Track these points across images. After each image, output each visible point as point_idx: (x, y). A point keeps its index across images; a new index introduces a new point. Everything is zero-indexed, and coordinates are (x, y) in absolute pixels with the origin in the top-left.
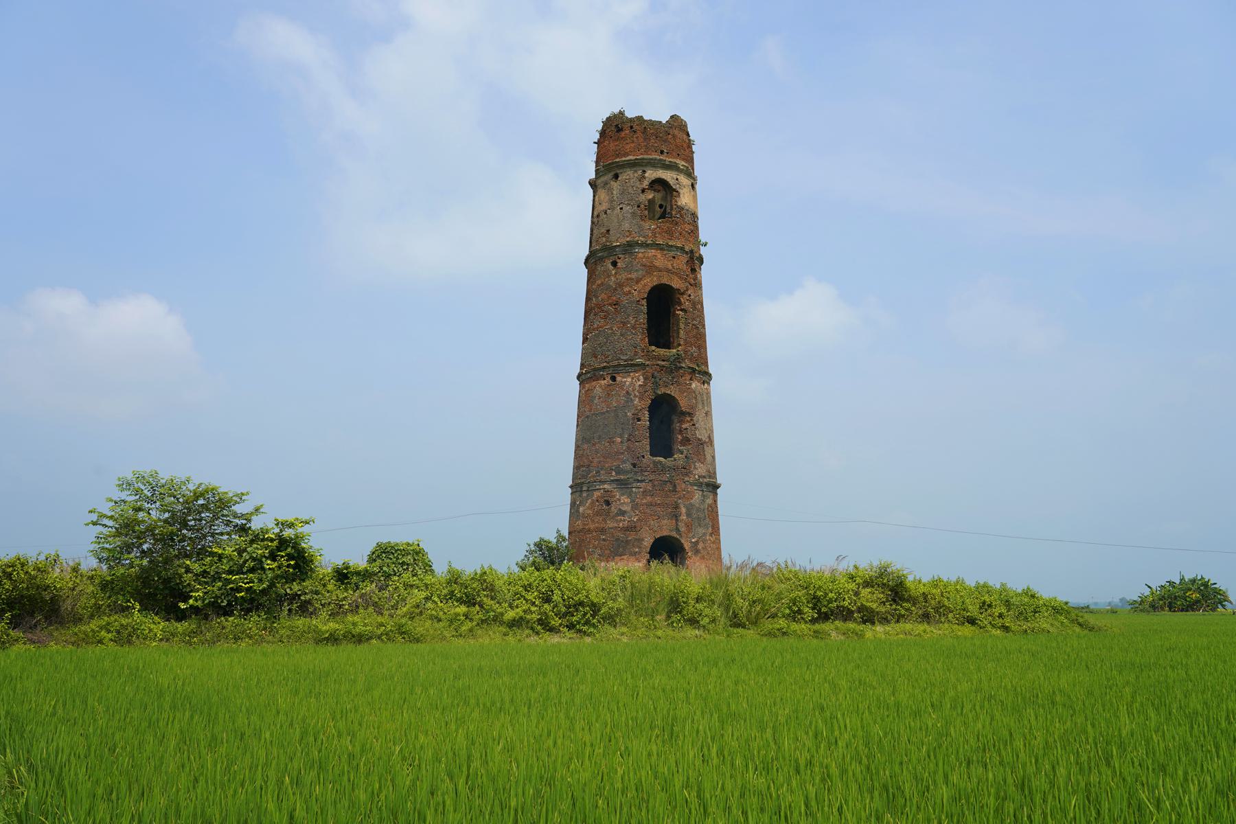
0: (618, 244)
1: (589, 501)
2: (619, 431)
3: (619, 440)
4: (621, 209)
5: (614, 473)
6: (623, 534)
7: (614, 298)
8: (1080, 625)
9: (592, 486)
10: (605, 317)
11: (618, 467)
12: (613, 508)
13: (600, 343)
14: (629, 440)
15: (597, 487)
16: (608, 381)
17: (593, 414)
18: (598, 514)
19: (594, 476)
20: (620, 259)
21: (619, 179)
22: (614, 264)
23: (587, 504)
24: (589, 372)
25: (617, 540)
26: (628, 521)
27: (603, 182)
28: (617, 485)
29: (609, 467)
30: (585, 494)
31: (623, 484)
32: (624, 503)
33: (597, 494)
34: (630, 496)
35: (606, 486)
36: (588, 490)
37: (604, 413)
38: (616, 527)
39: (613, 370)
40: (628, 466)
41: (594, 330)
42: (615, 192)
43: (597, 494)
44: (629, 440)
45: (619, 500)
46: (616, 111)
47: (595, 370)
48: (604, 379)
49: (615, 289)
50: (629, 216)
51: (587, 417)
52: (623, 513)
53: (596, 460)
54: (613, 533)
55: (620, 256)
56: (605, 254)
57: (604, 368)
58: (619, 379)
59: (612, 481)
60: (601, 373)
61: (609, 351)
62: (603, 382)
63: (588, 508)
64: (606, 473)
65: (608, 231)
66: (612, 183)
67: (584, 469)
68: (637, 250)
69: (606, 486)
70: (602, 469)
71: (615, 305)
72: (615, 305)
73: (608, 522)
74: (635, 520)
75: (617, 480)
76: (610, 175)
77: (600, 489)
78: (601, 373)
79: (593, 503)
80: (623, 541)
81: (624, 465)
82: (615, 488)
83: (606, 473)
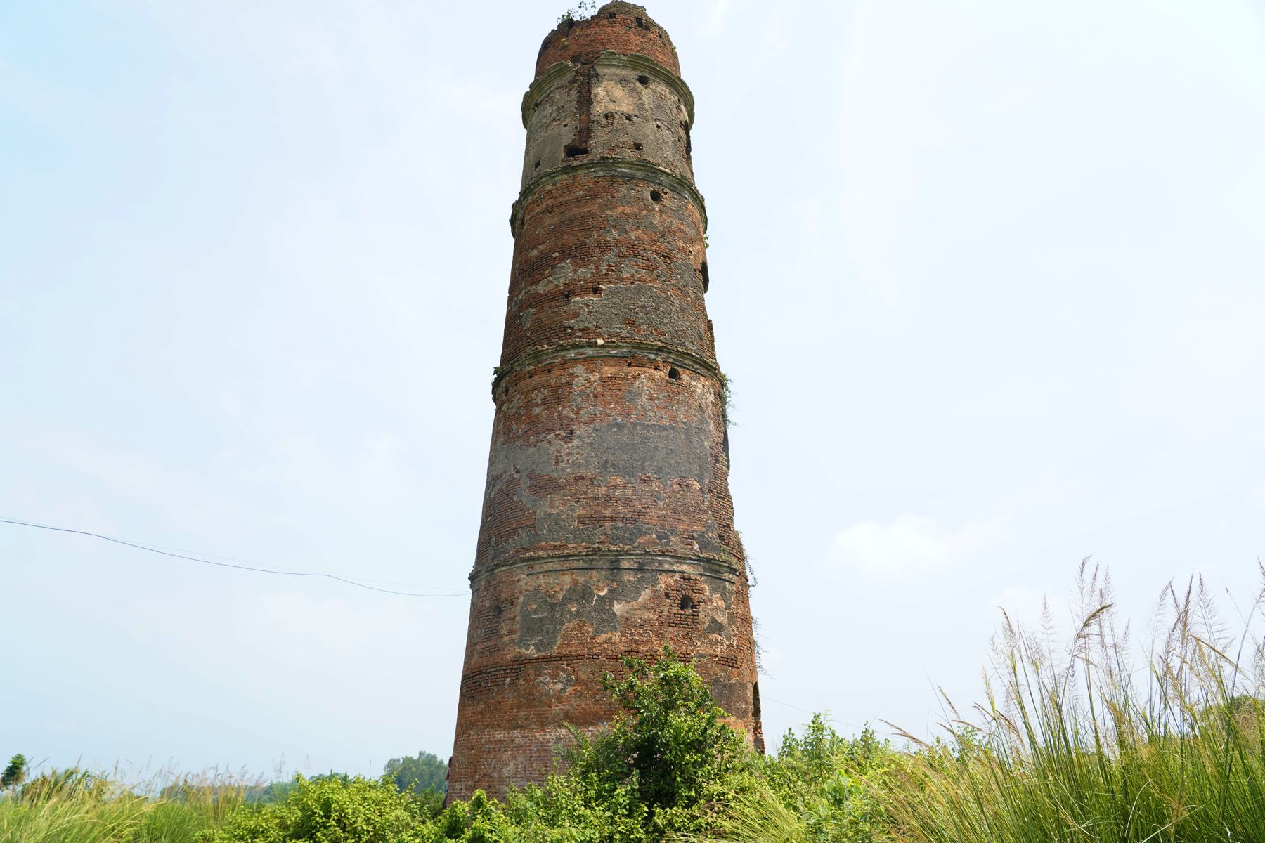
0: (668, 171)
1: (645, 594)
2: (695, 468)
3: (696, 485)
4: (658, 127)
5: (696, 546)
6: (723, 670)
7: (663, 247)
8: (92, 829)
9: (652, 562)
10: (650, 269)
11: (702, 535)
12: (702, 615)
13: (644, 306)
14: (710, 491)
15: (666, 566)
16: (662, 374)
17: (635, 425)
18: (672, 622)
19: (654, 543)
20: (666, 193)
21: (651, 86)
22: (656, 196)
23: (640, 599)
24: (616, 347)
25: (716, 681)
26: (728, 646)
27: (617, 75)
28: (705, 569)
29: (685, 530)
30: (628, 577)
31: (712, 570)
32: (716, 608)
33: (664, 582)
34: (723, 597)
35: (684, 567)
36: (641, 569)
37: (664, 428)
38: (711, 656)
39: (674, 359)
40: (713, 536)
41: (621, 279)
42: (645, 99)
43: (664, 582)
44: (710, 491)
45: (710, 600)
46: (639, 4)
47: (638, 346)
48: (656, 368)
49: (663, 235)
50: (671, 143)
51: (620, 427)
52: (717, 627)
53: (654, 512)
54: (707, 668)
55: (666, 190)
56: (639, 174)
57: (660, 350)
58: (685, 377)
59: (700, 560)
60: (652, 356)
61: (665, 325)
62: (657, 374)
63: (644, 607)
64: (682, 542)
65: (638, 147)
66: (638, 84)
67: (620, 524)
68: (687, 196)
69: (684, 567)
70: (672, 532)
71: (663, 256)
72: (663, 256)
73: (696, 642)
74: (735, 644)
75: (707, 560)
76: (632, 74)
77: (674, 572)
78: (652, 356)
79: (655, 598)
80: (724, 686)
81: (710, 535)
82: (701, 575)
83: (682, 542)
